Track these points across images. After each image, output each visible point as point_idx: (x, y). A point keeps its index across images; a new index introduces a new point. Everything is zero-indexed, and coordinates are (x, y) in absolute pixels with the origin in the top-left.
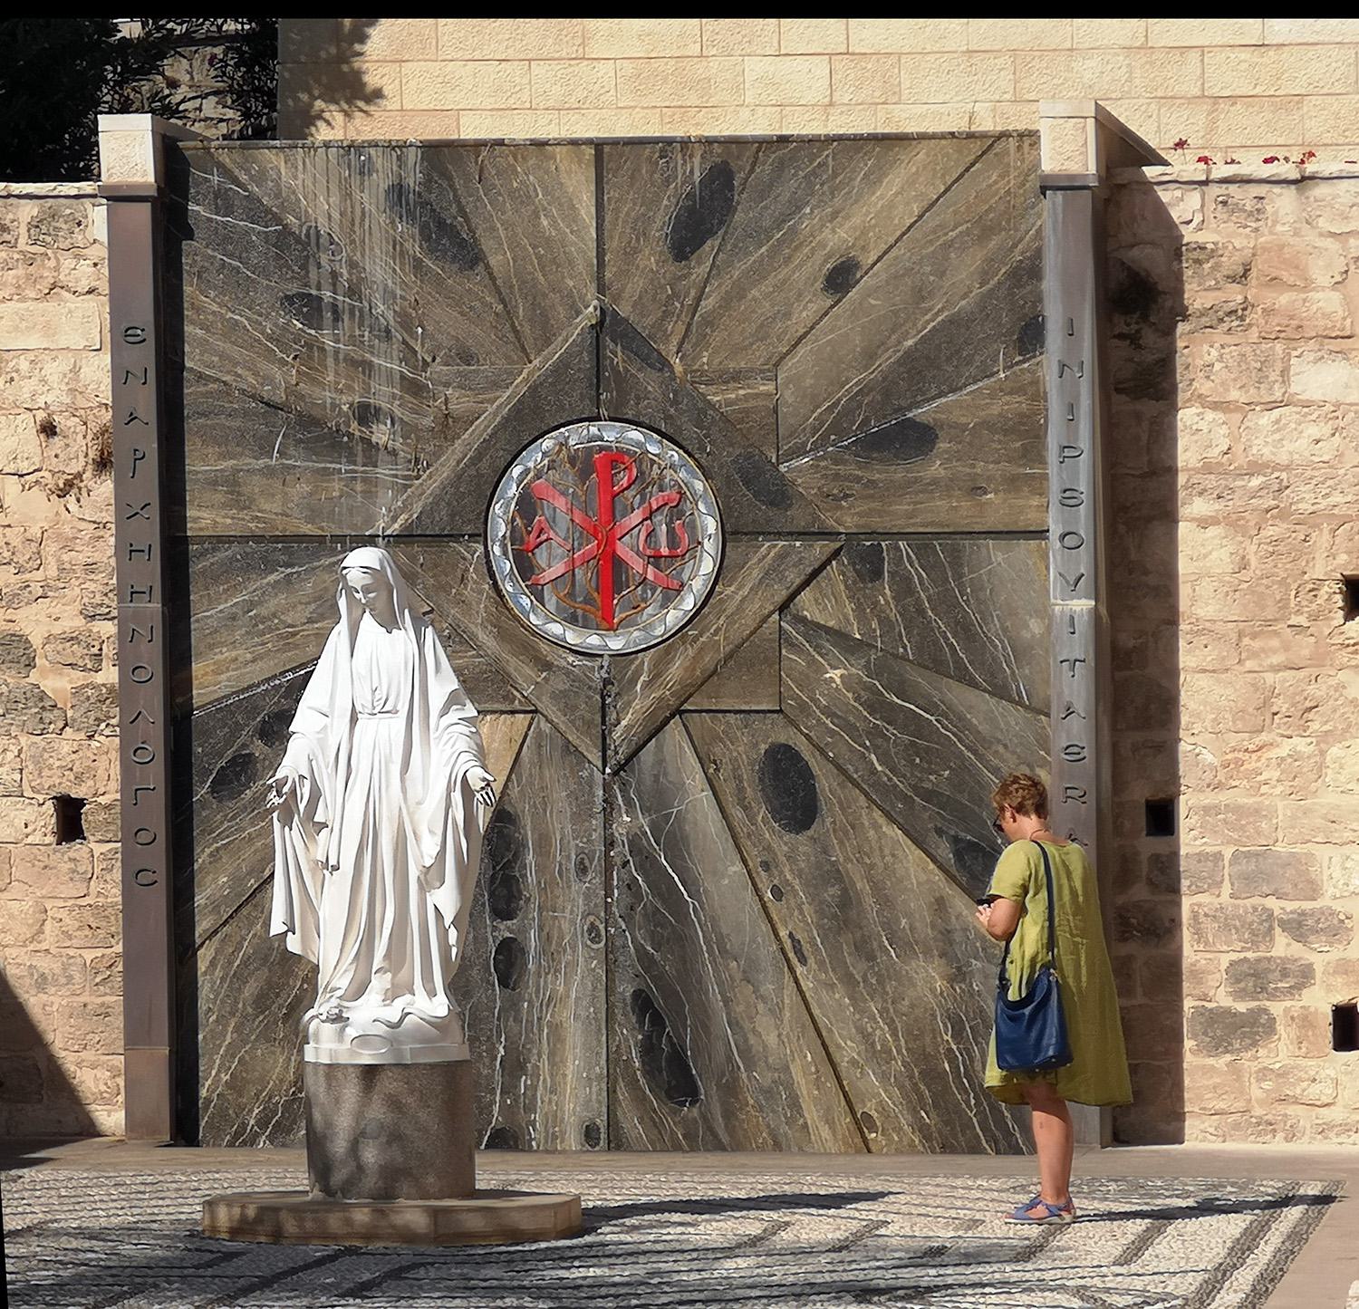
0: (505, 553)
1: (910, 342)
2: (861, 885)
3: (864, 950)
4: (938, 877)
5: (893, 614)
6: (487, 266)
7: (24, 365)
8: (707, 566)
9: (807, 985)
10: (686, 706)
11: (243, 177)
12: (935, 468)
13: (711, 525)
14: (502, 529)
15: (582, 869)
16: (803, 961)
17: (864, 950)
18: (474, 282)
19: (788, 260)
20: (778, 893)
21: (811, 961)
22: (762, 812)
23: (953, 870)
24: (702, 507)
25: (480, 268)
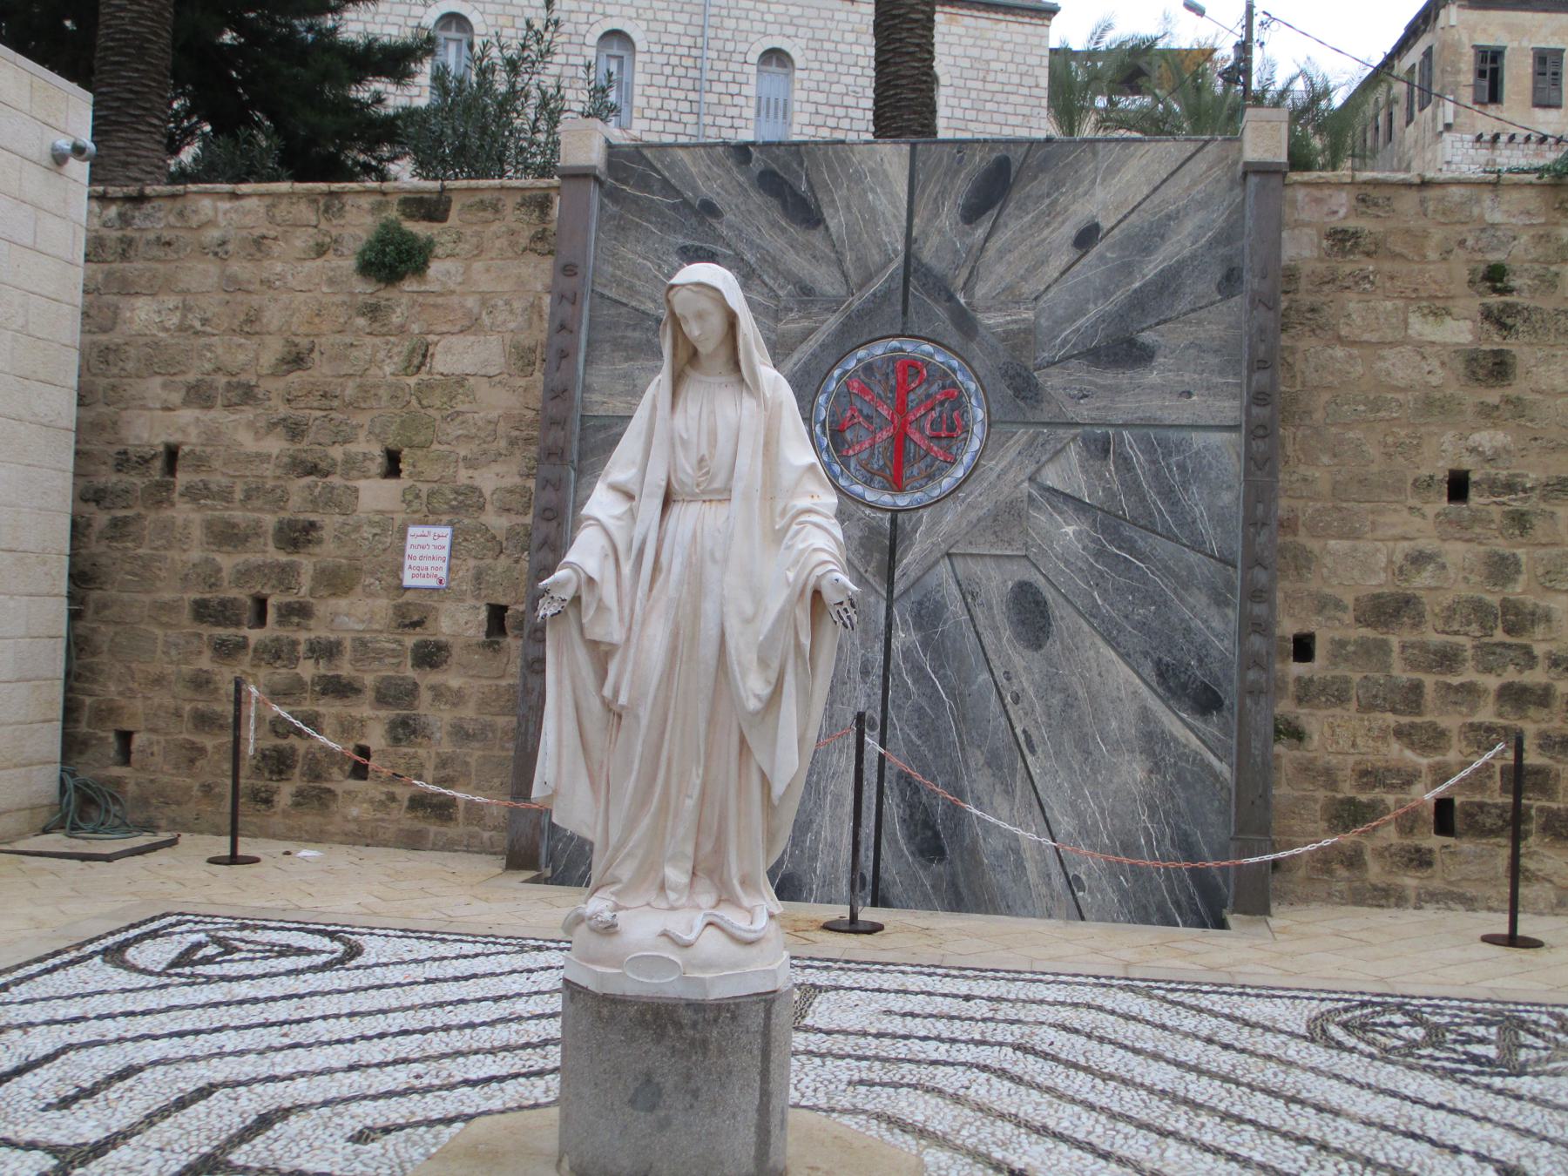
0: (824, 432)
1: (1137, 285)
2: (1081, 693)
3: (1083, 745)
4: (1144, 690)
5: (1116, 486)
6: (827, 228)
7: (500, 303)
8: (976, 444)
9: (1035, 771)
10: (953, 551)
11: (659, 166)
12: (1154, 377)
13: (980, 414)
14: (823, 414)
15: (865, 672)
16: (1033, 751)
17: (1083, 745)
18: (816, 237)
19: (1048, 224)
20: (1017, 699)
21: (1039, 751)
22: (1007, 634)
23: (1155, 685)
24: (973, 401)
25: (822, 227)
